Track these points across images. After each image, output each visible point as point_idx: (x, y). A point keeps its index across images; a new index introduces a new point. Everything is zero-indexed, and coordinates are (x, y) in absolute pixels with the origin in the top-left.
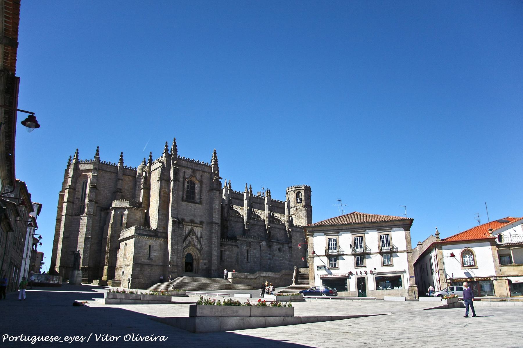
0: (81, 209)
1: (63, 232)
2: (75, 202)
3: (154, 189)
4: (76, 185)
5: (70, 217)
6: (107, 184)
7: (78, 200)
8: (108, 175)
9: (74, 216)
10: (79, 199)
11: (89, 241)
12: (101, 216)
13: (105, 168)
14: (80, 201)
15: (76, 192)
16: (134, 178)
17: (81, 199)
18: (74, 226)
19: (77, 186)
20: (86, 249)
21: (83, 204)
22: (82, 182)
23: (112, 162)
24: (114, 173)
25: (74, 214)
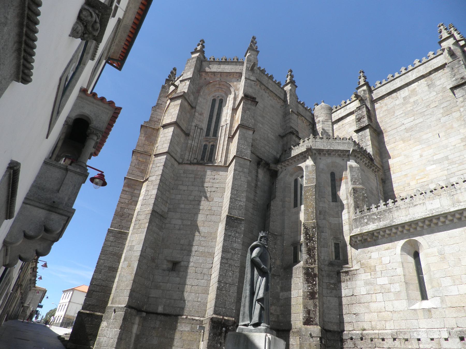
0: (204, 152)
1: (154, 196)
2: (191, 134)
3: (403, 127)
4: (196, 98)
5: (176, 164)
6: (268, 114)
7: (199, 130)
8: (270, 98)
9: (187, 164)
10: (201, 129)
11: (238, 230)
12: (257, 176)
13: (265, 80)
14: (204, 134)
15: (197, 114)
16: (309, 125)
17: (205, 130)
18: (185, 188)
19: (199, 101)
20: (229, 256)
21: (212, 143)
22: (210, 99)
23: (277, 78)
24: (280, 98)
25: (188, 160)
